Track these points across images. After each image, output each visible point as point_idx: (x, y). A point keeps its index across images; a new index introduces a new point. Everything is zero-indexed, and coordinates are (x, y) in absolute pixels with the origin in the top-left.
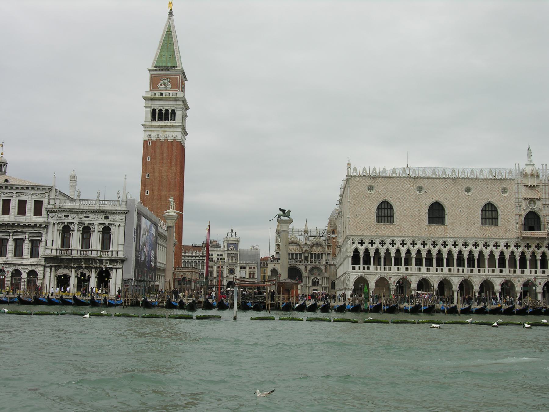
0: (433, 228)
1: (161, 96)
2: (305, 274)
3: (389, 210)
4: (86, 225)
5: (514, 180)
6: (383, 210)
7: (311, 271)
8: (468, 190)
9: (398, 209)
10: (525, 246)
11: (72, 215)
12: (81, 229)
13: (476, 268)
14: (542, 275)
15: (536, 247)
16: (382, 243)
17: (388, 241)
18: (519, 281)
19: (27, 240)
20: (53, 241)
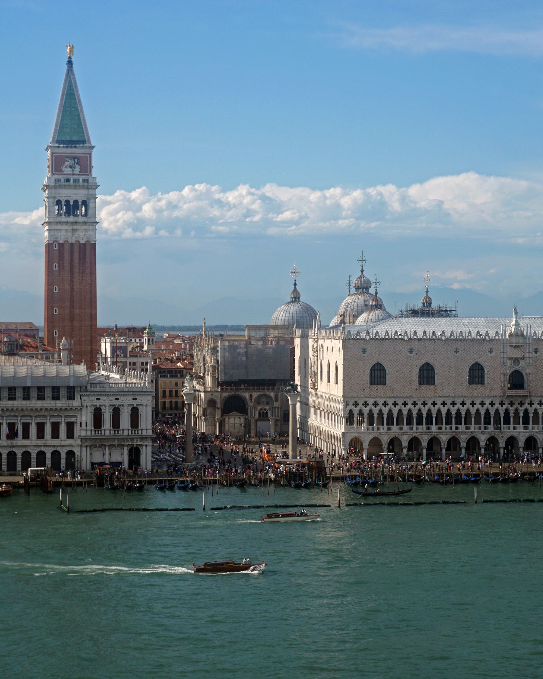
0: (423, 388)
1: (68, 183)
2: (251, 404)
3: (382, 372)
4: (117, 406)
5: (500, 340)
6: (376, 371)
7: (258, 401)
8: (457, 351)
9: (390, 371)
10: (509, 404)
11: (102, 398)
12: (111, 410)
13: (463, 426)
14: (524, 431)
15: (519, 404)
16: (376, 404)
17: (381, 402)
18: (503, 437)
19: (63, 423)
20: (86, 423)
